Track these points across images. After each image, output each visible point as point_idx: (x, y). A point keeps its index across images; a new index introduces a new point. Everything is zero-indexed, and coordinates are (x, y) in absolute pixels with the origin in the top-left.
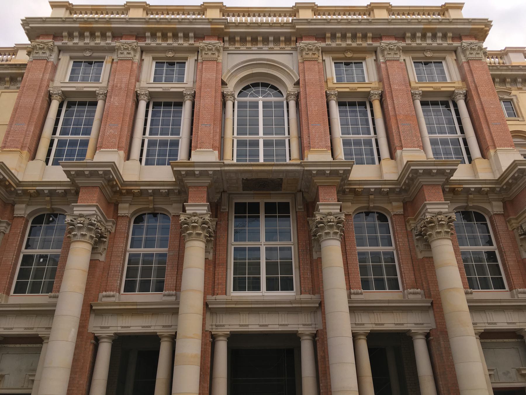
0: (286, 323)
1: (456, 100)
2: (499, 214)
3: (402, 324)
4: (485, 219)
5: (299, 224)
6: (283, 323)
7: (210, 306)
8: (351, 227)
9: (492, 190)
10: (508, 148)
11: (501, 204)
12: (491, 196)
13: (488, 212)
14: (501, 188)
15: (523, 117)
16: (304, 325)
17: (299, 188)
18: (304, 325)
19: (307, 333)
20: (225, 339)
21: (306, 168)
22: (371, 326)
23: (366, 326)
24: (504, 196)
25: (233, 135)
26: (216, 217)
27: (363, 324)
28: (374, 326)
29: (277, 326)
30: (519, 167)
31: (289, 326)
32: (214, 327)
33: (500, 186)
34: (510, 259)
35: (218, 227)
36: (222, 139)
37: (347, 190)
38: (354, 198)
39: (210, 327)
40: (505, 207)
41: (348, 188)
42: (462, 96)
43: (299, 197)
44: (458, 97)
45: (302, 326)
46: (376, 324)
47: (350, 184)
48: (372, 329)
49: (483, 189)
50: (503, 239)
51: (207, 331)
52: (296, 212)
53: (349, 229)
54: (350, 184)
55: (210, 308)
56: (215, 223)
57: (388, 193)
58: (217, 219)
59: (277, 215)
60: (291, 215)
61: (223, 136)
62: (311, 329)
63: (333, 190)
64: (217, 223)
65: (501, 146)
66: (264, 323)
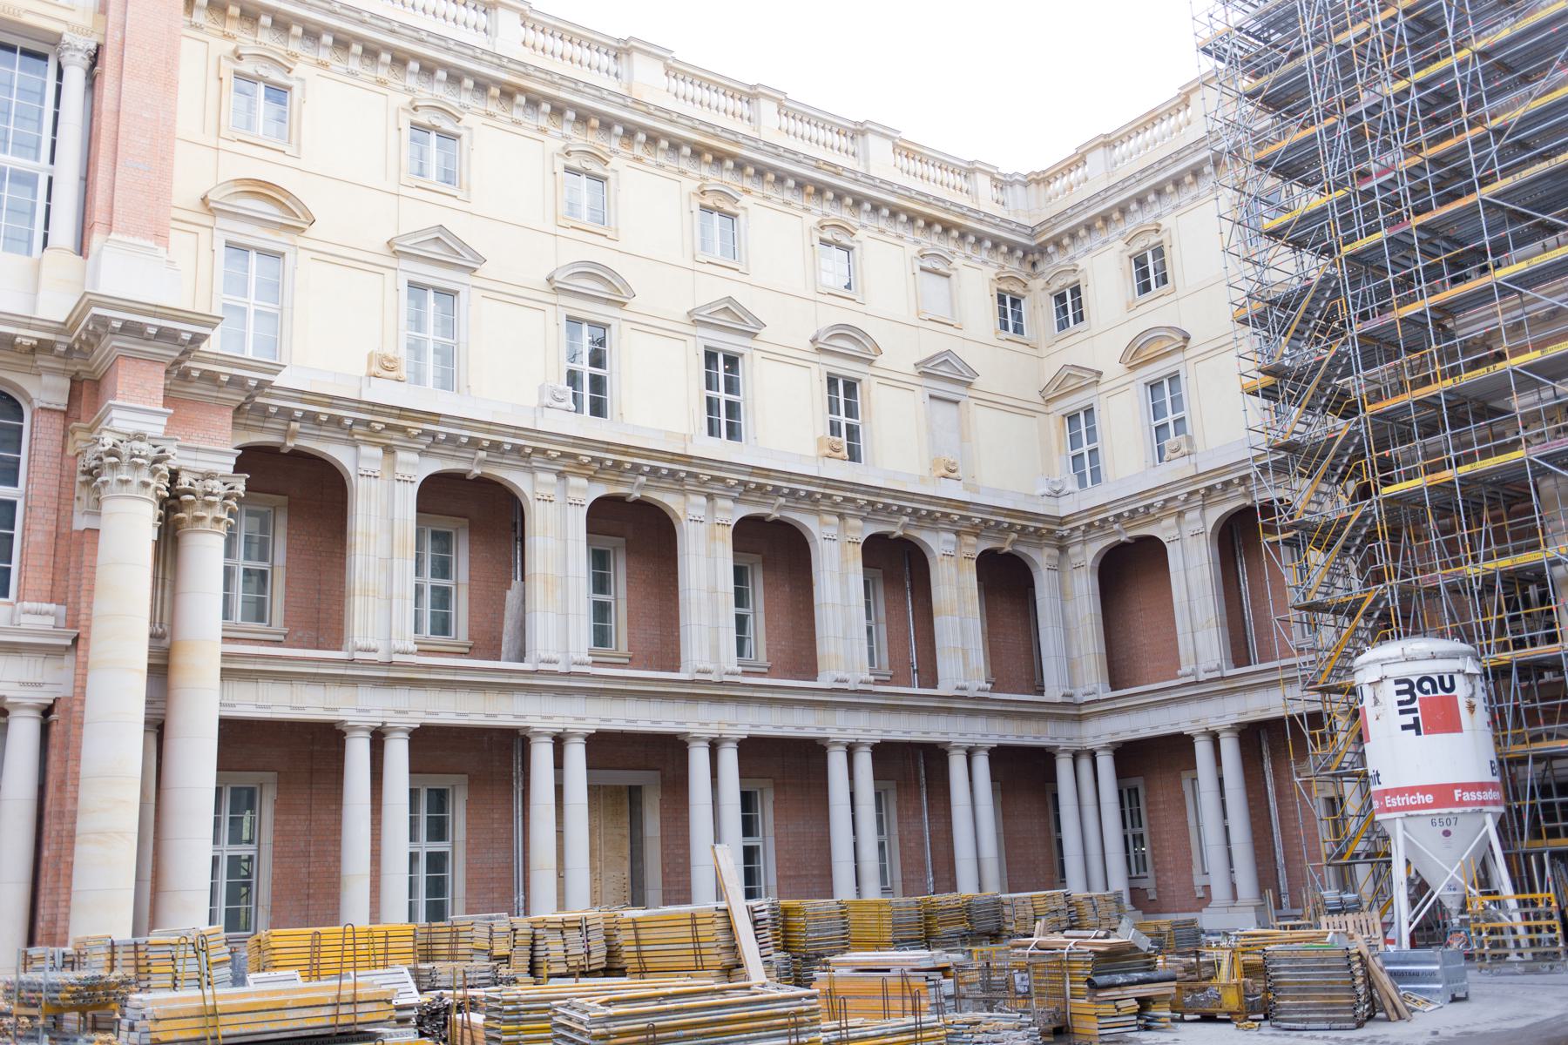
1: (63, 62)
2: (55, 411)
4: (22, 415)
9: (43, 347)
10: (142, 242)
11: (66, 384)
12: (43, 361)
13: (30, 402)
14: (70, 349)
15: (299, 145)
24: (79, 367)
30: (95, 310)
33: (70, 340)
34: (39, 527)
40: (74, 395)
42: (79, 55)
44: (67, 54)
49: (18, 340)
50: (40, 475)
65: (126, 231)
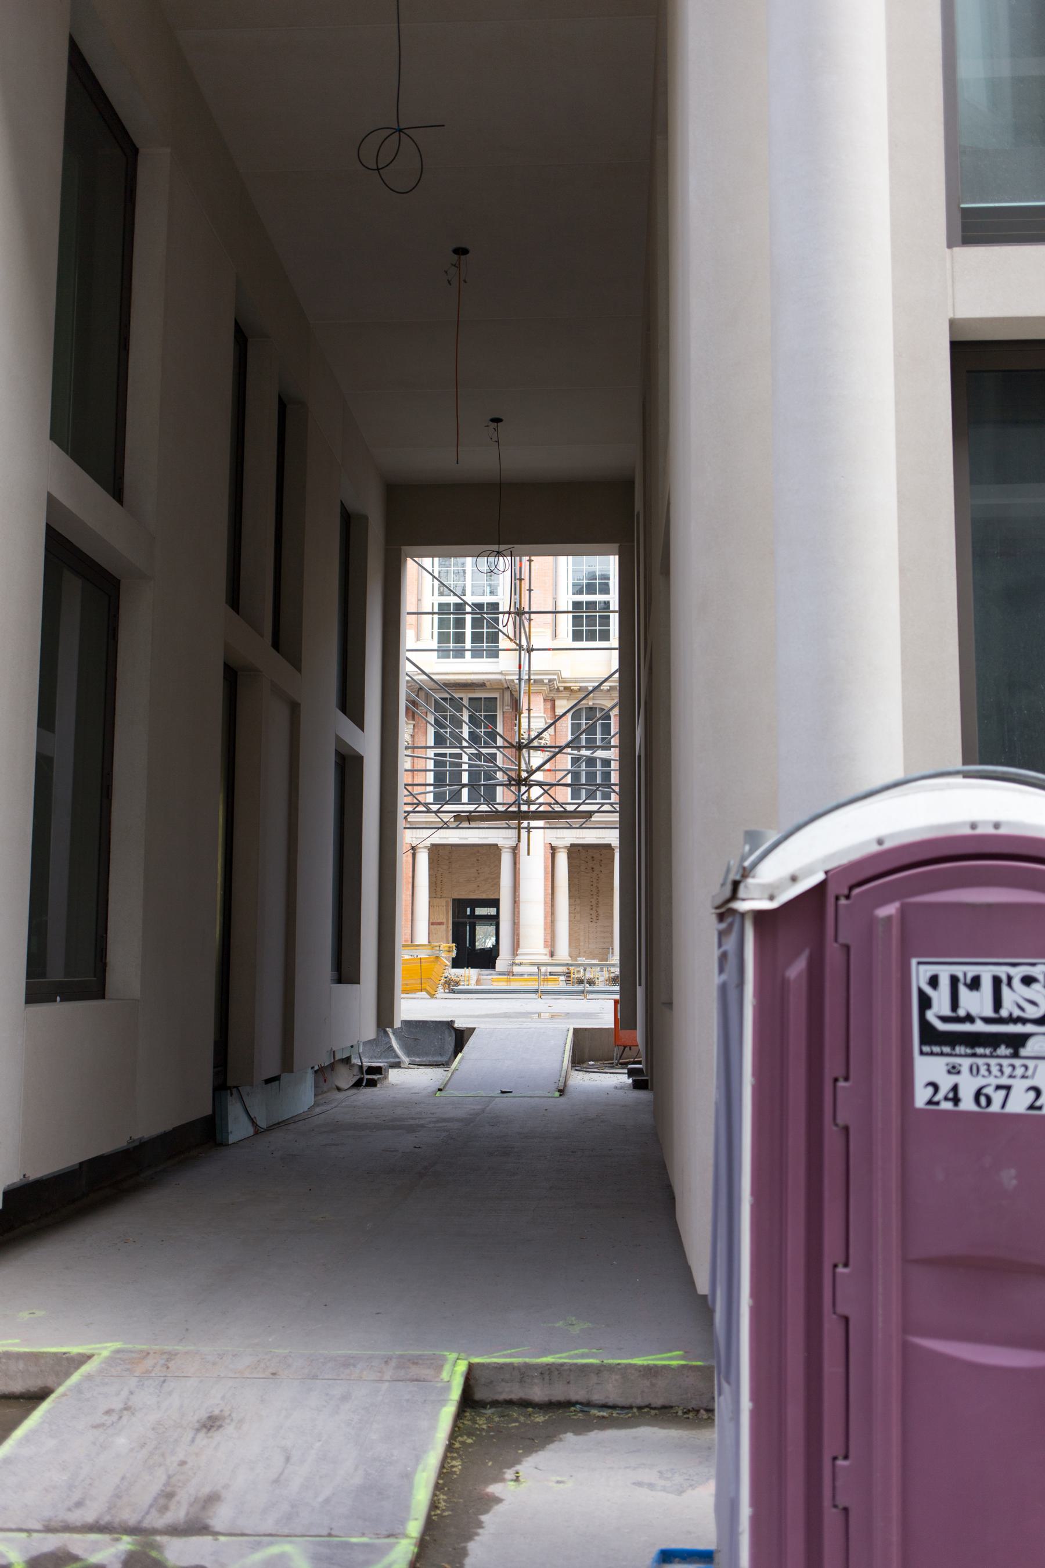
0: (487, 836)
5: (505, 727)
6: (484, 836)
7: (409, 820)
16: (504, 838)
17: (506, 686)
18: (504, 838)
19: (507, 846)
20: (426, 850)
21: (508, 677)
22: (572, 839)
23: (566, 839)
25: (433, 595)
26: (413, 719)
27: (564, 838)
28: (575, 839)
29: (477, 839)
31: (489, 839)
32: (414, 839)
35: (415, 730)
36: (419, 602)
38: (570, 695)
39: (411, 839)
43: (507, 695)
45: (501, 839)
48: (572, 842)
51: (407, 843)
52: (503, 712)
53: (561, 733)
55: (409, 822)
56: (412, 727)
57: (609, 690)
58: (414, 722)
59: (483, 713)
60: (498, 714)
62: (511, 843)
63: (538, 698)
64: (414, 726)
66: (464, 836)
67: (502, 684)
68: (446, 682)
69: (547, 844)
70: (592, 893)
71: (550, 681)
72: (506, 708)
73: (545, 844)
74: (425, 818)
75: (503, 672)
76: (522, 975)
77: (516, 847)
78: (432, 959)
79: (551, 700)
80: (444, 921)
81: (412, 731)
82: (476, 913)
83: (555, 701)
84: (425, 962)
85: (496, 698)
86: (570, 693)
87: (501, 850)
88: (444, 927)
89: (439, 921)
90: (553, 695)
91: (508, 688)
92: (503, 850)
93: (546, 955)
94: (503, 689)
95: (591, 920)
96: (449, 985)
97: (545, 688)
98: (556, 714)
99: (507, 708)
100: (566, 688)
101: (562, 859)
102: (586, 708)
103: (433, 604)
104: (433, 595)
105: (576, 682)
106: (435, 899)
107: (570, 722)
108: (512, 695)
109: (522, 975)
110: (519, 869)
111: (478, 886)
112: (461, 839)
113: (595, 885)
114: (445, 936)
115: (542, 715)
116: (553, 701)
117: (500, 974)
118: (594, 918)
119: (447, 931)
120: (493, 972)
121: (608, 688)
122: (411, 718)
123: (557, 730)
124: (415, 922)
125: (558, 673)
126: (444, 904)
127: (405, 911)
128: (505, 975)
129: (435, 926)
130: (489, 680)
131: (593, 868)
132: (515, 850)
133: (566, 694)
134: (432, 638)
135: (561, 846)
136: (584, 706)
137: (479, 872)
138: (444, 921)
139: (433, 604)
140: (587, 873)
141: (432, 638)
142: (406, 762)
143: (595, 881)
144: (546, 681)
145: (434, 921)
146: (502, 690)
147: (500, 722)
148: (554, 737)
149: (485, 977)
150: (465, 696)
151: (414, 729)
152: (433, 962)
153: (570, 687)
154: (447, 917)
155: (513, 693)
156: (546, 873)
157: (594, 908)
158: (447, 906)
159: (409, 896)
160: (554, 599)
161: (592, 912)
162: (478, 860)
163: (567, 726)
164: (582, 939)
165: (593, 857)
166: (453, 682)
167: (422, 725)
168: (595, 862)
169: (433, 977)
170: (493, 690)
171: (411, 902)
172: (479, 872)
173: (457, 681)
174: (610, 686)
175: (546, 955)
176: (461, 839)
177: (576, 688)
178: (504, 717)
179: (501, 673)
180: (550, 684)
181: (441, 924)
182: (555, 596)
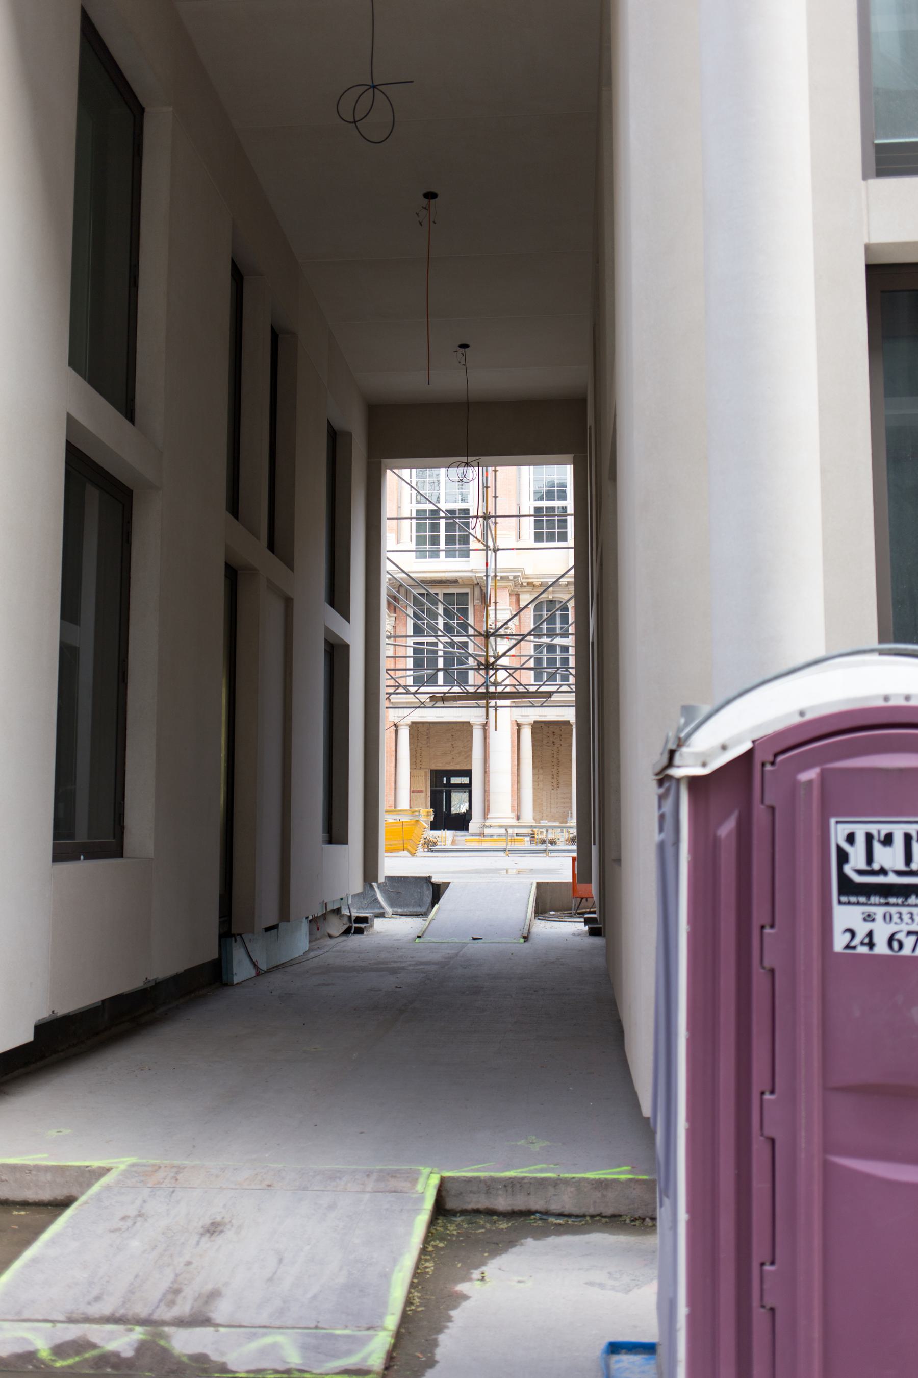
0: (460, 715)
3: (563, 715)
5: (476, 619)
6: (458, 715)
7: (392, 701)
8: (528, 621)
16: (475, 716)
17: (476, 583)
18: (475, 716)
20: (407, 728)
21: (477, 575)
25: (411, 503)
26: (395, 612)
27: (528, 716)
29: (452, 717)
32: (396, 718)
35: (397, 622)
36: (399, 509)
37: (525, 584)
38: (533, 590)
41: (525, 582)
43: (477, 591)
46: (540, 716)
47: (527, 578)
48: (536, 720)
51: (390, 721)
52: (474, 606)
54: (527, 578)
55: (392, 702)
57: (567, 585)
58: (395, 615)
59: (456, 607)
60: (469, 607)
61: (399, 506)
62: (482, 720)
64: (396, 618)
67: (472, 580)
68: (423, 579)
69: (513, 721)
70: (553, 764)
71: (515, 577)
72: (477, 601)
73: (511, 721)
74: (406, 699)
75: (474, 570)
76: (492, 836)
77: (486, 724)
78: (413, 823)
79: (516, 594)
80: (424, 789)
81: (394, 622)
82: (452, 782)
83: (519, 595)
84: (407, 825)
85: (467, 593)
86: (532, 588)
87: (473, 727)
88: (423, 795)
89: (419, 789)
90: (517, 590)
91: (478, 584)
92: (475, 727)
93: (513, 818)
94: (473, 585)
95: (553, 788)
96: (428, 845)
97: (510, 584)
98: (520, 607)
99: (477, 602)
100: (529, 584)
101: (527, 734)
102: (546, 601)
103: (411, 510)
104: (411, 503)
105: (538, 578)
106: (415, 770)
107: (532, 613)
108: (481, 590)
109: (492, 836)
110: (489, 743)
111: (453, 759)
112: (437, 717)
113: (555, 756)
114: (424, 802)
115: (509, 607)
116: (518, 595)
117: (472, 836)
118: (555, 785)
119: (426, 797)
120: (466, 834)
121: (566, 583)
122: (393, 611)
123: (521, 621)
124: (397, 790)
125: (521, 570)
126: (423, 774)
127: (389, 781)
128: (477, 836)
129: (415, 794)
130: (461, 578)
131: (553, 742)
132: (485, 726)
133: (529, 589)
134: (411, 541)
135: (525, 723)
136: (545, 600)
137: (454, 746)
138: (424, 789)
139: (411, 510)
140: (549, 746)
141: (411, 541)
142: (389, 650)
143: (555, 753)
144: (511, 578)
145: (414, 789)
146: (472, 586)
147: (471, 614)
148: (518, 627)
149: (459, 838)
150: (440, 591)
151: (395, 621)
152: (413, 825)
153: (533, 582)
154: (425, 786)
155: (482, 588)
156: (512, 746)
157: (555, 777)
158: (426, 776)
159: (392, 768)
160: (518, 505)
161: (553, 781)
162: (452, 736)
163: (530, 617)
164: (544, 804)
165: (554, 733)
166: (429, 579)
167: (402, 617)
168: (555, 736)
169: (413, 839)
170: (464, 586)
171: (394, 772)
172: (454, 746)
173: (433, 579)
174: (568, 582)
175: (513, 818)
176: (437, 717)
177: (537, 584)
178: (474, 610)
179: (472, 571)
180: (515, 580)
181: (421, 791)
182: (518, 503)
